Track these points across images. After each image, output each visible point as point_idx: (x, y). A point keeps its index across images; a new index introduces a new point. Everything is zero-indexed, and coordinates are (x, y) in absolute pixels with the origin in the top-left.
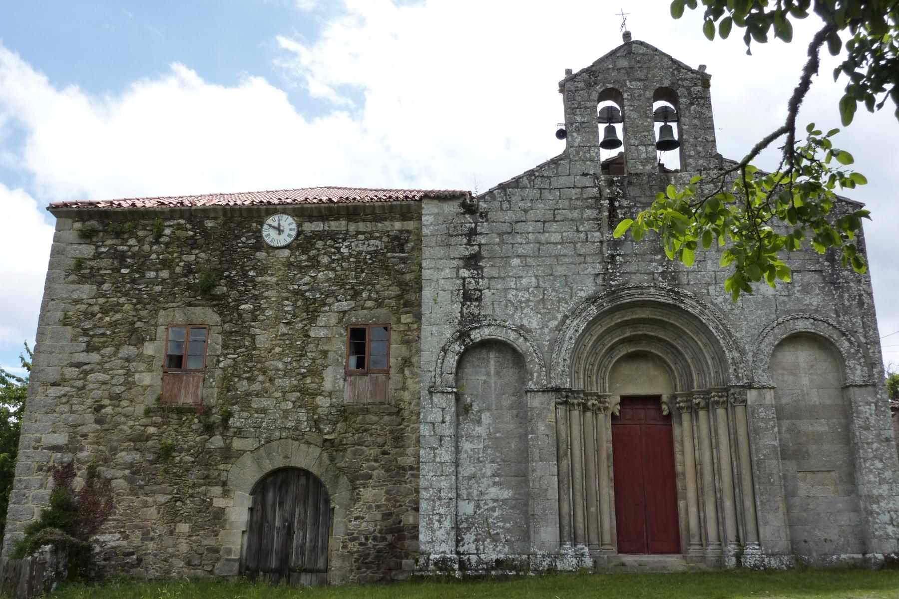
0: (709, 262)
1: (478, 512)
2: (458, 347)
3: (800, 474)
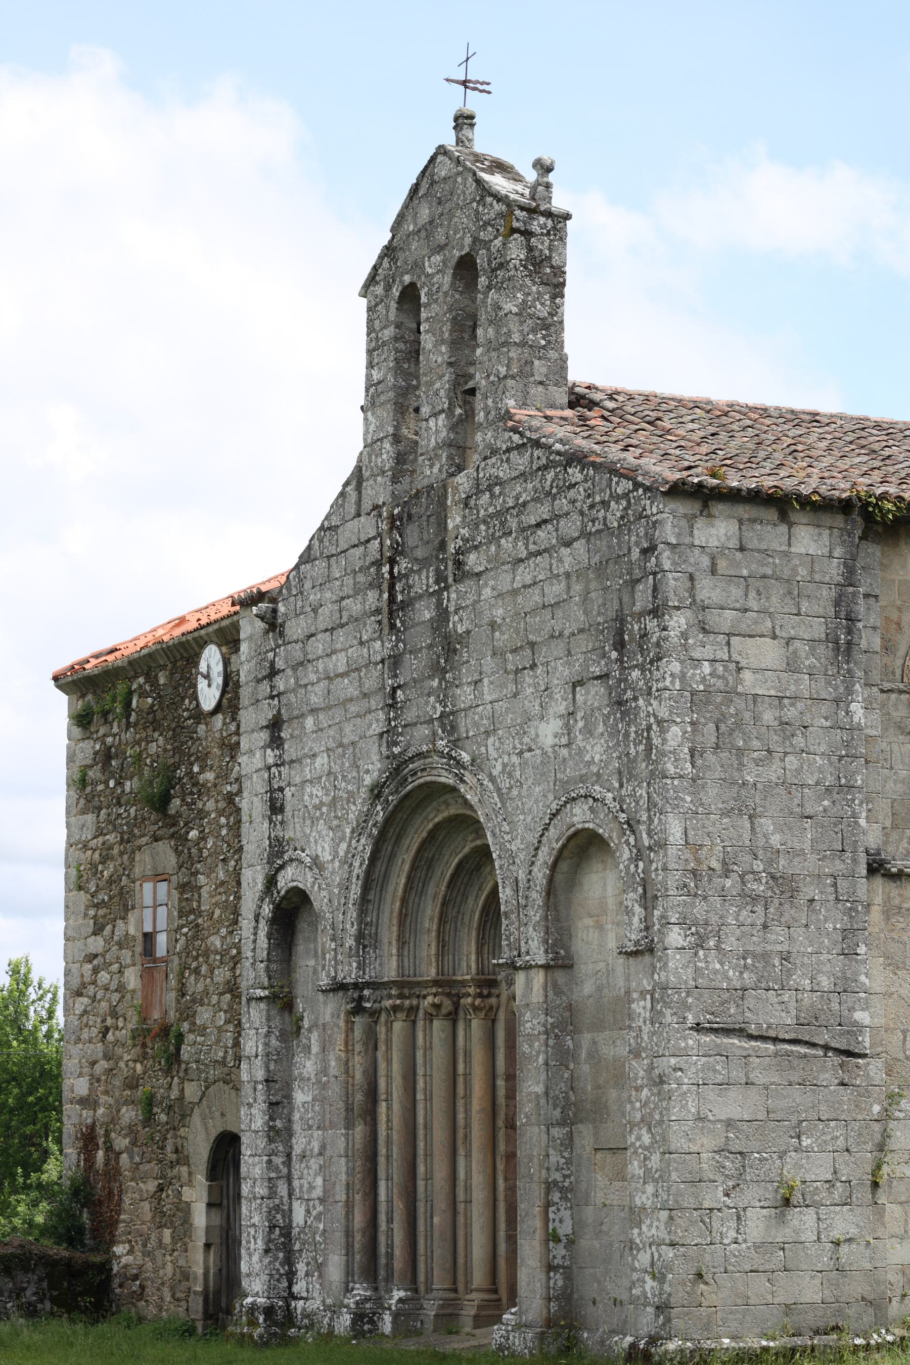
0: (486, 681)
1: (309, 1223)
2: (267, 910)
3: (599, 1155)
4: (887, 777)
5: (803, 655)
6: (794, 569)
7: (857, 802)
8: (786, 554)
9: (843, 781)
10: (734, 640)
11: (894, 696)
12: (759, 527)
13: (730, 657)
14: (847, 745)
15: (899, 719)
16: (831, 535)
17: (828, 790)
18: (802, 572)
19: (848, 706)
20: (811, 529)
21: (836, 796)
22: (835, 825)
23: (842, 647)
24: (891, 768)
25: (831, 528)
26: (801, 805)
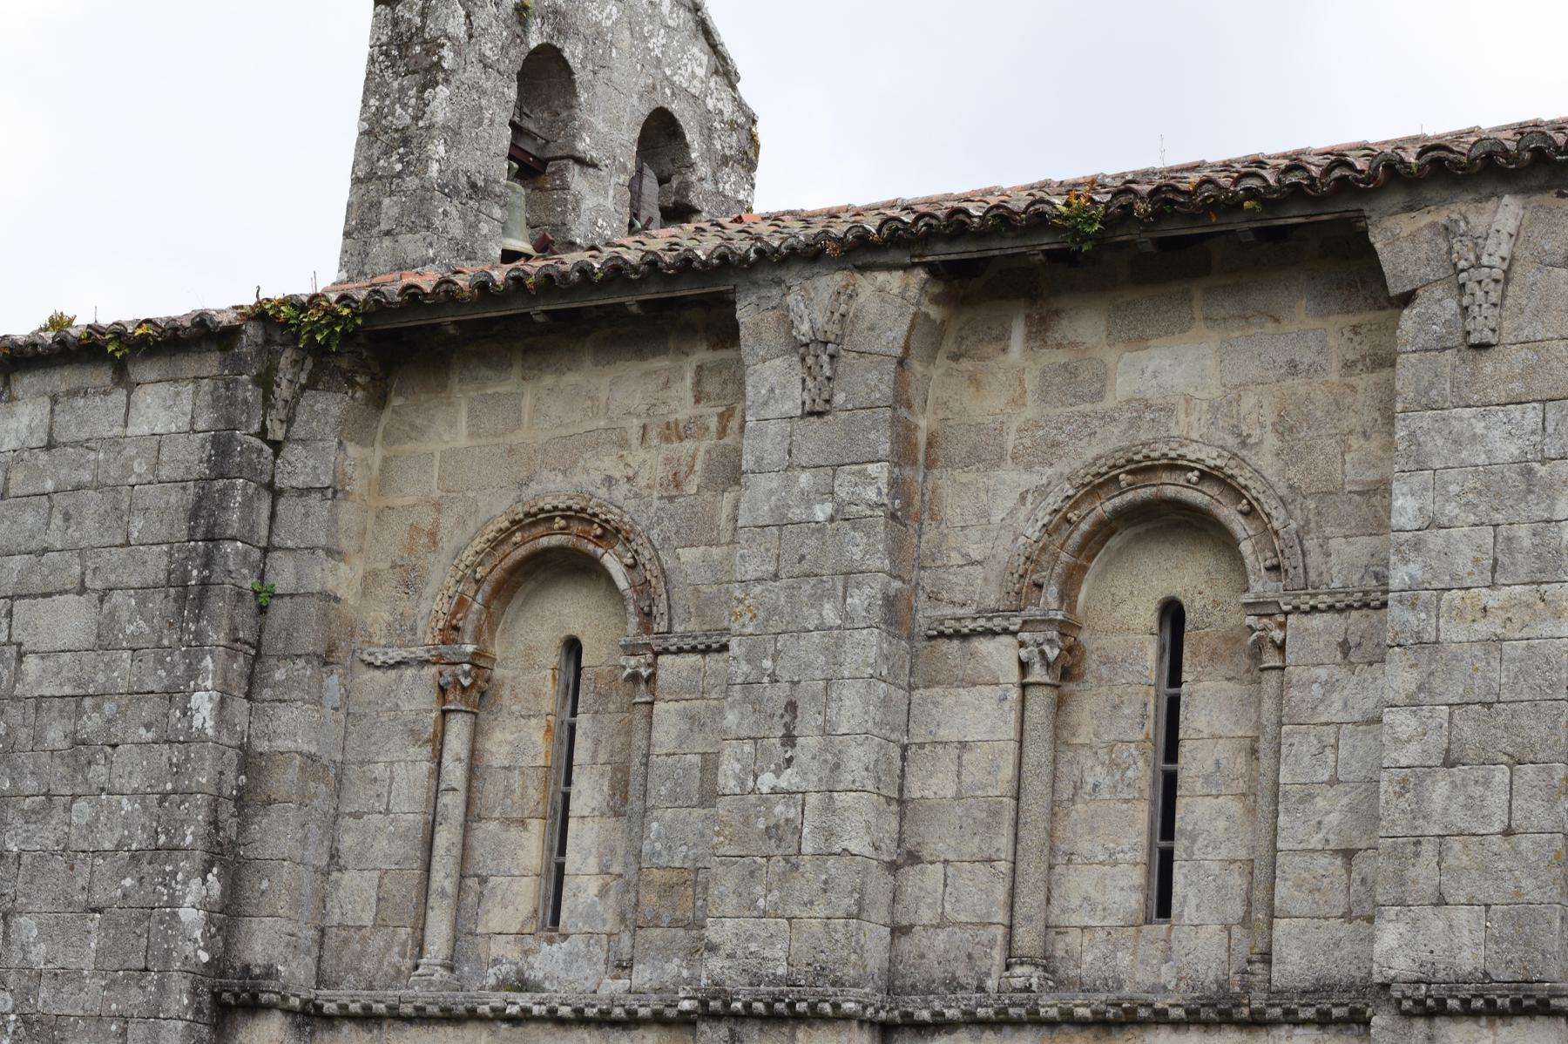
4: (378, 829)
5: (124, 615)
6: (127, 468)
7: (180, 877)
8: (116, 441)
9: (162, 839)
10: (20, 606)
11: (409, 673)
12: (81, 402)
13: (10, 636)
14: (177, 770)
15: (412, 717)
16: (196, 393)
17: (135, 857)
18: (140, 467)
19: (188, 699)
20: (165, 389)
21: (146, 868)
22: (139, 922)
23: (190, 596)
24: (388, 811)
25: (196, 379)
26: (87, 889)
